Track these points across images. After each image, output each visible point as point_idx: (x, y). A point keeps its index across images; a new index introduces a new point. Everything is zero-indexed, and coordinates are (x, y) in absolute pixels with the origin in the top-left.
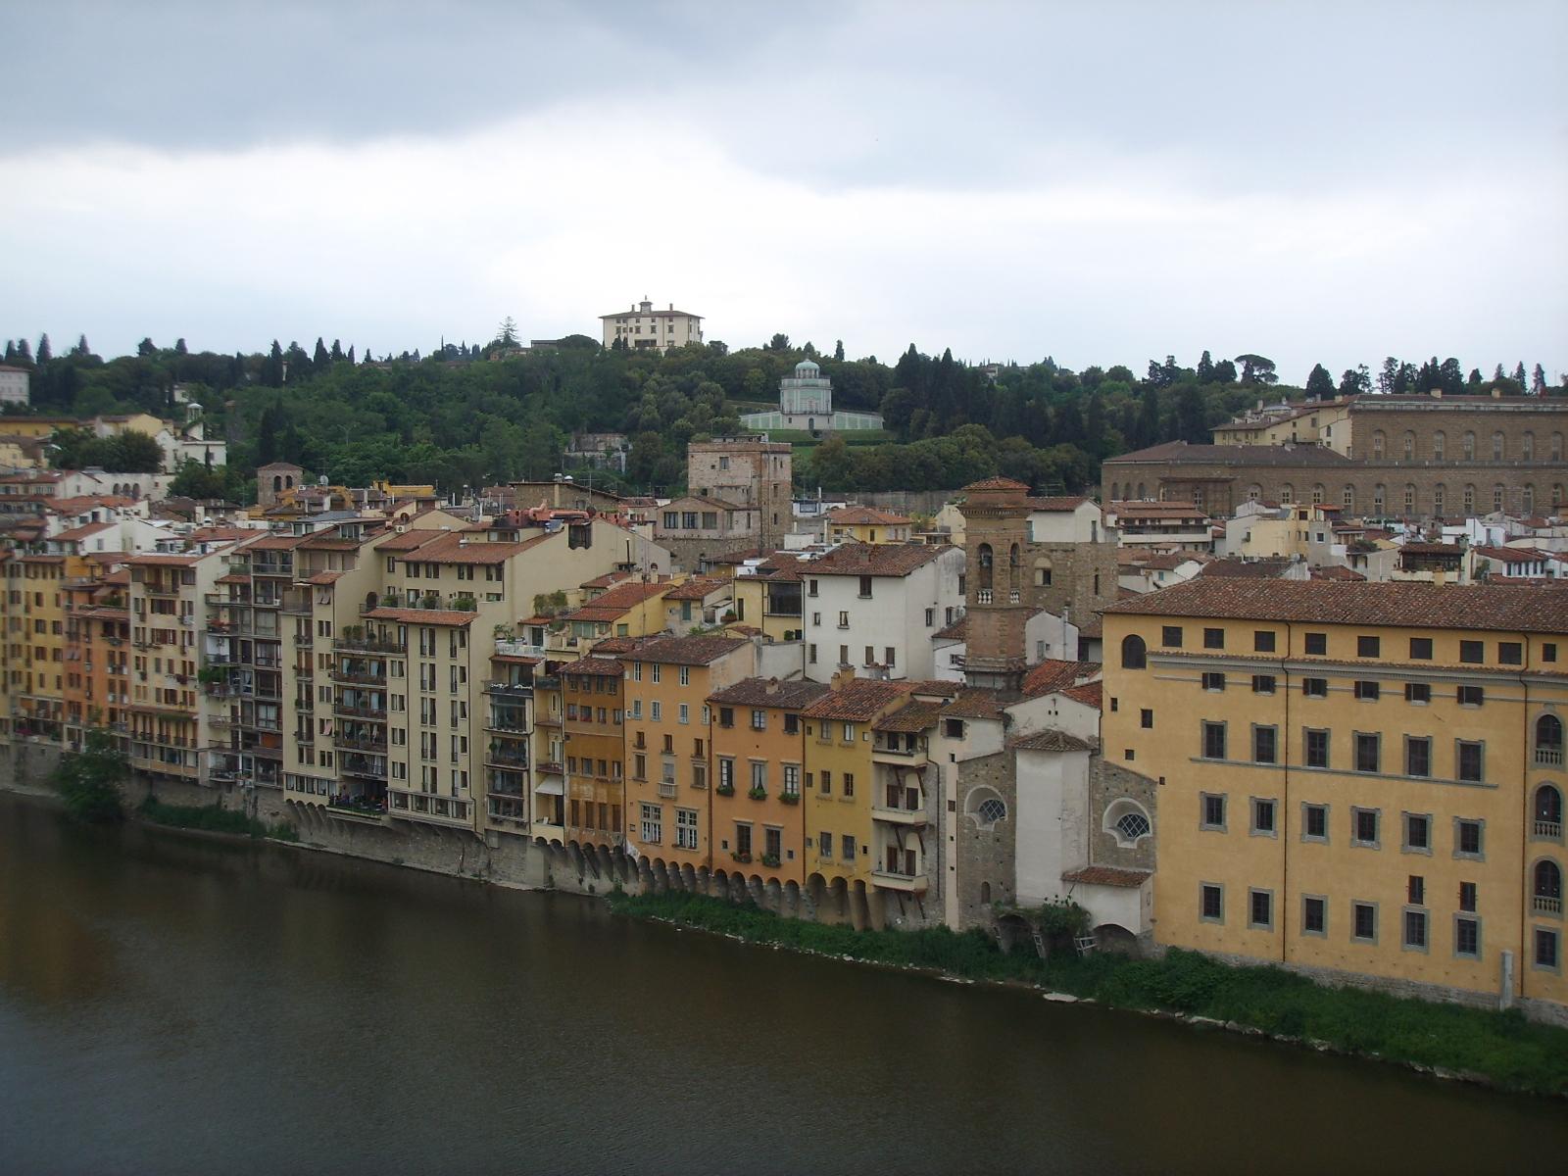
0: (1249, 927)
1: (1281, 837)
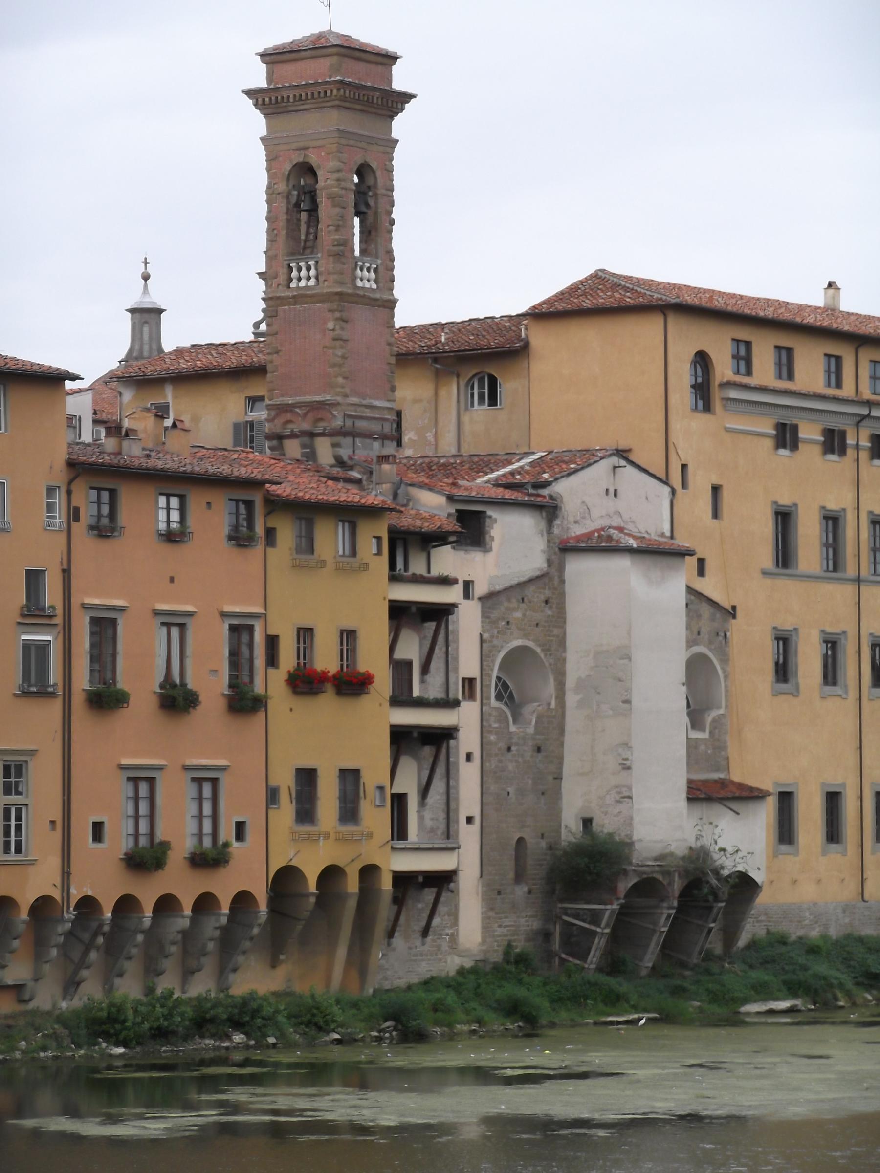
0: (824, 853)
1: (853, 694)
